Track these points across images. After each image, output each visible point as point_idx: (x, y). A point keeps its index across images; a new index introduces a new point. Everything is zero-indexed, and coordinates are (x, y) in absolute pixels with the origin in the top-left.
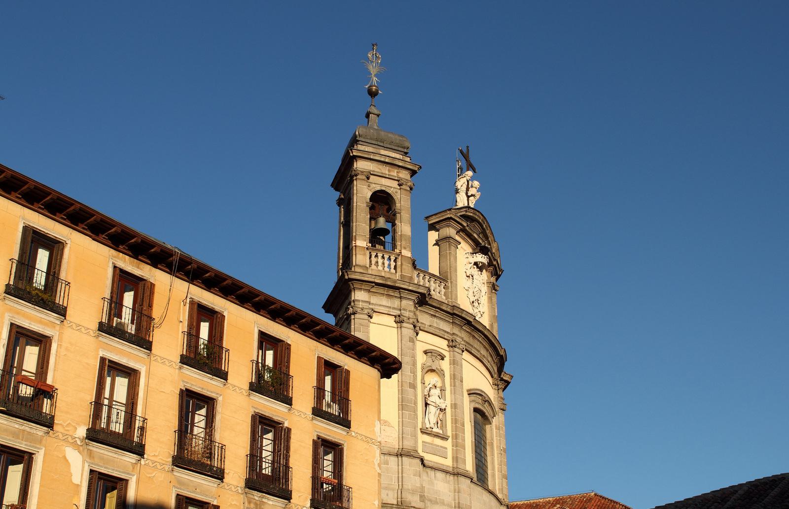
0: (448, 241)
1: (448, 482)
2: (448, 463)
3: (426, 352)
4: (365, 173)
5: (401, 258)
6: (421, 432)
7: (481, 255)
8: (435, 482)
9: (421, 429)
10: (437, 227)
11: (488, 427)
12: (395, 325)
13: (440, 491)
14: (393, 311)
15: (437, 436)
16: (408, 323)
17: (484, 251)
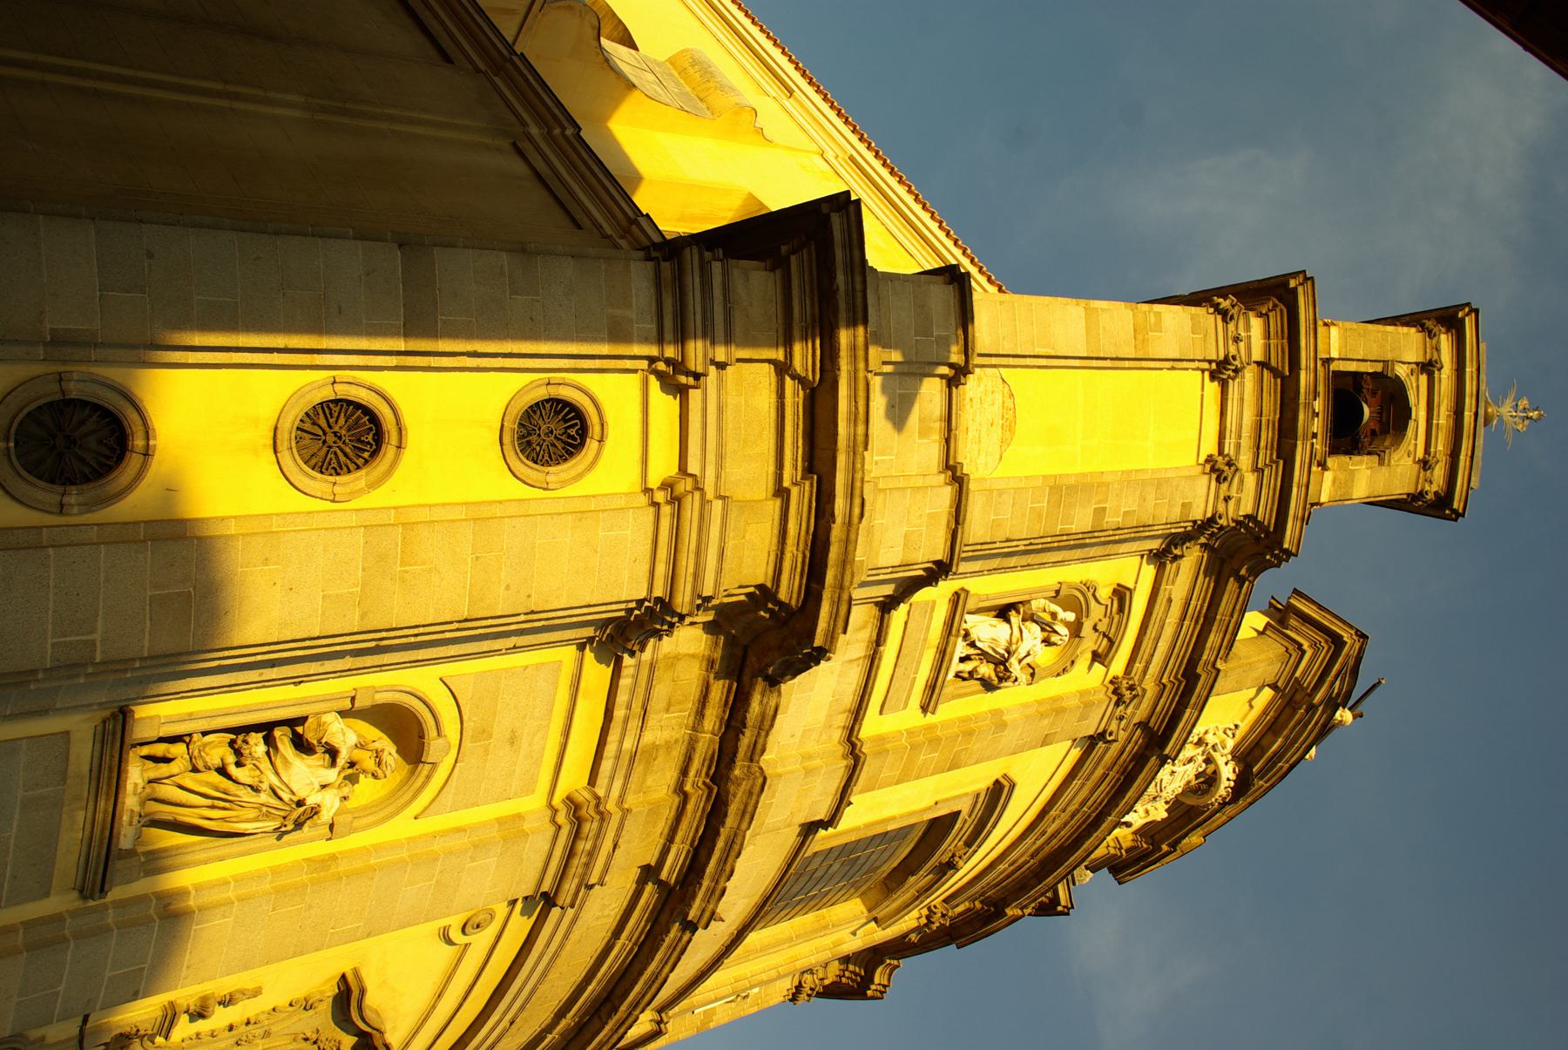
0: (1291, 648)
1: (828, 726)
3: (1122, 595)
6: (957, 594)
7: (1233, 777)
9: (963, 589)
10: (1293, 622)
11: (853, 908)
12: (1202, 459)
14: (1232, 446)
15: (943, 654)
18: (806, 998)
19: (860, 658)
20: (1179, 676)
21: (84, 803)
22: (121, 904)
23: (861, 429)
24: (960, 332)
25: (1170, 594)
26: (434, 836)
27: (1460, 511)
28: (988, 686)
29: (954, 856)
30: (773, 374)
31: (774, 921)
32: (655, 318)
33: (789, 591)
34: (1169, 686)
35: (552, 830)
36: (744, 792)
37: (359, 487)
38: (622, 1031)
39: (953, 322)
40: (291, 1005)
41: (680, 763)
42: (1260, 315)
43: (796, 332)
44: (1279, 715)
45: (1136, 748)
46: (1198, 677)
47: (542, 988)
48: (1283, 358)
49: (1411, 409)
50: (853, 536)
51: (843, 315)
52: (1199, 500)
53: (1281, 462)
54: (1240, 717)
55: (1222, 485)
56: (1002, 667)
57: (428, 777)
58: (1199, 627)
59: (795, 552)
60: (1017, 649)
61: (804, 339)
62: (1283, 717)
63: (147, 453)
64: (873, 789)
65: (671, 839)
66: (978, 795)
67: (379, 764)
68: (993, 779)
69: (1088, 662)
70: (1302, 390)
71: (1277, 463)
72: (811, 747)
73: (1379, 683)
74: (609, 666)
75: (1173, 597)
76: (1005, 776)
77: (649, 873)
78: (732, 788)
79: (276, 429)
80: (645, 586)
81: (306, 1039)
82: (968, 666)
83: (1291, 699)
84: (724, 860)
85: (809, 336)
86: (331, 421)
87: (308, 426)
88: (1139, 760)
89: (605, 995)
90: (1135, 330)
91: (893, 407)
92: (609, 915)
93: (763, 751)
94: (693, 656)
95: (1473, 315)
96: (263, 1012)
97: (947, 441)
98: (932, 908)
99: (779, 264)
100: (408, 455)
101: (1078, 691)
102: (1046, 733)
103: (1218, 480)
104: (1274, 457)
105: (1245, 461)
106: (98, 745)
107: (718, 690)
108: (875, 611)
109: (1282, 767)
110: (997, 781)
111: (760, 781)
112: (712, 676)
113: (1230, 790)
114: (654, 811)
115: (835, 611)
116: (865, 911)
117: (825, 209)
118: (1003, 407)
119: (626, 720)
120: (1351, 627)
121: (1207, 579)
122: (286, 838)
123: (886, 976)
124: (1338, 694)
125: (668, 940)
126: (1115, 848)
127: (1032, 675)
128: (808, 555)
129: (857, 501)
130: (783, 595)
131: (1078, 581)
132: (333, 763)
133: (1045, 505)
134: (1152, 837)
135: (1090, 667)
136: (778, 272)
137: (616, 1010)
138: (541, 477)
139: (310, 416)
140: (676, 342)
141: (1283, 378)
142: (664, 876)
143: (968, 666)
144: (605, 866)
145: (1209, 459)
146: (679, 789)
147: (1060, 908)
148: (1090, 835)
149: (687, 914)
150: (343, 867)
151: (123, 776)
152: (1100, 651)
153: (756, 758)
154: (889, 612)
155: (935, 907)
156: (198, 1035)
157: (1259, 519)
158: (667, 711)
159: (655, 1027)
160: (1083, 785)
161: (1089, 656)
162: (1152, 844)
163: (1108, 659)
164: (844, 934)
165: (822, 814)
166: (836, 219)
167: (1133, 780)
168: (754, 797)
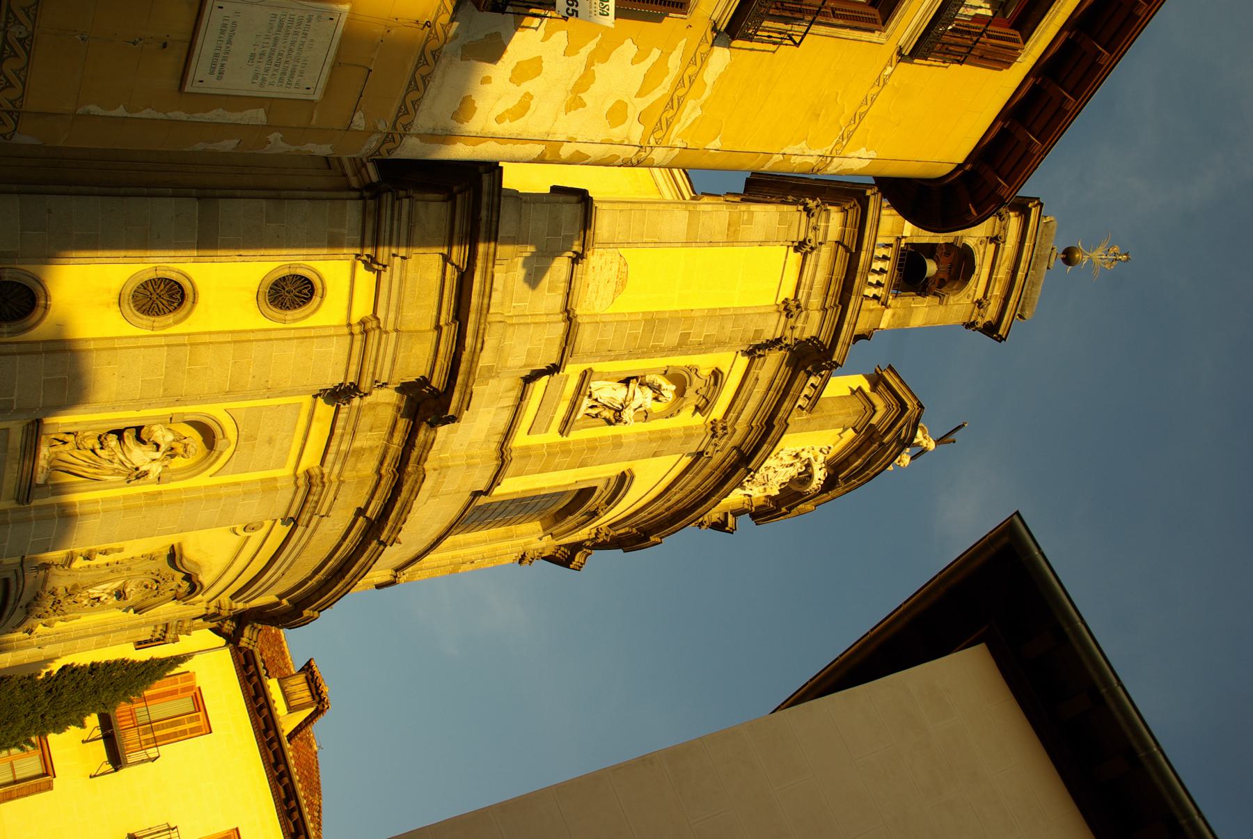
0: (867, 407)
1: (487, 440)
2: (521, 439)
3: (717, 374)
4: (1002, 232)
5: (877, 310)
7: (823, 478)
8: (493, 410)
9: (590, 369)
10: (880, 388)
11: (536, 526)
12: (779, 301)
13: (474, 422)
14: (805, 294)
15: (574, 406)
16: (785, 326)
17: (829, 484)
18: (528, 563)
19: (509, 406)
20: (763, 424)
21: (18, 461)
22: (38, 508)
23: (486, 301)
24: (582, 233)
25: (758, 375)
26: (220, 486)
27: (1004, 337)
28: (609, 422)
29: (598, 508)
30: (441, 260)
31: (477, 529)
32: (360, 233)
33: (438, 381)
34: (755, 429)
35: (293, 488)
36: (413, 480)
37: (169, 323)
38: (348, 587)
39: (578, 227)
40: (142, 557)
41: (380, 457)
42: (843, 210)
43: (456, 239)
44: (862, 444)
45: (733, 460)
46: (774, 426)
47: (298, 561)
48: (853, 241)
49: (975, 267)
50: (475, 359)
51: (482, 234)
52: (772, 327)
53: (840, 307)
54: (833, 442)
55: (790, 320)
56: (618, 414)
57: (218, 458)
58: (779, 396)
59: (443, 360)
60: (629, 405)
61: (460, 244)
62: (864, 446)
63: (46, 307)
64: (521, 475)
65: (372, 497)
66: (609, 479)
67: (186, 451)
68: (622, 471)
69: (693, 411)
70: (861, 264)
71: (837, 307)
72: (474, 451)
73: (963, 425)
74: (333, 406)
75: (760, 377)
76: (629, 470)
77: (360, 512)
78: (406, 477)
79: (120, 294)
80: (343, 377)
81: (152, 573)
82: (594, 411)
83: (871, 436)
84: (401, 513)
85: (463, 242)
86: (155, 287)
87: (142, 290)
88: (734, 468)
89: (339, 568)
90: (729, 225)
91: (530, 275)
92: (338, 529)
93: (426, 460)
94: (388, 404)
95: (1039, 207)
96: (126, 559)
97: (568, 294)
98: (599, 529)
99: (451, 198)
100: (198, 307)
101: (683, 427)
102: (655, 450)
103: (787, 316)
104: (837, 303)
105: (816, 302)
106: (25, 435)
107: (402, 424)
108: (521, 382)
109: (868, 474)
110: (623, 473)
111: (422, 476)
112: (399, 415)
113: (820, 486)
114: (361, 481)
115: (462, 398)
116: (541, 530)
117: (481, 169)
118: (619, 271)
119: (342, 435)
120: (916, 398)
121: (787, 368)
122: (132, 482)
123: (583, 558)
124: (905, 438)
125: (370, 548)
126: (748, 505)
127: (646, 417)
128: (450, 364)
129: (480, 340)
130: (434, 383)
131: (684, 365)
132: (158, 450)
133: (641, 331)
134: (777, 501)
135: (693, 414)
136: (449, 203)
137: (343, 577)
138: (282, 316)
139: (145, 285)
140: (372, 246)
141: (851, 253)
142: (368, 514)
143: (594, 411)
144: (329, 507)
145: (786, 301)
146: (378, 471)
147: (727, 529)
148: (701, 506)
149: (380, 538)
150: (165, 498)
151: (37, 451)
152: (700, 405)
153: (421, 463)
154: (529, 383)
155: (601, 529)
156: (89, 566)
157: (820, 339)
158: (370, 431)
159: (393, 579)
160: (693, 478)
161: (694, 407)
162: (776, 506)
163: (704, 411)
164: (534, 538)
165: (482, 486)
166: (486, 179)
167: (730, 479)
168: (418, 484)
